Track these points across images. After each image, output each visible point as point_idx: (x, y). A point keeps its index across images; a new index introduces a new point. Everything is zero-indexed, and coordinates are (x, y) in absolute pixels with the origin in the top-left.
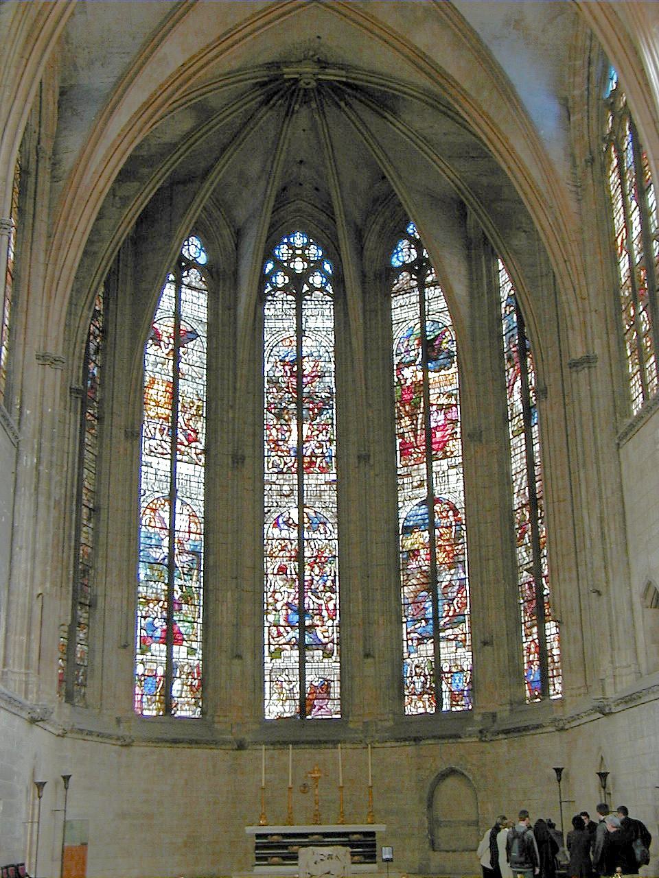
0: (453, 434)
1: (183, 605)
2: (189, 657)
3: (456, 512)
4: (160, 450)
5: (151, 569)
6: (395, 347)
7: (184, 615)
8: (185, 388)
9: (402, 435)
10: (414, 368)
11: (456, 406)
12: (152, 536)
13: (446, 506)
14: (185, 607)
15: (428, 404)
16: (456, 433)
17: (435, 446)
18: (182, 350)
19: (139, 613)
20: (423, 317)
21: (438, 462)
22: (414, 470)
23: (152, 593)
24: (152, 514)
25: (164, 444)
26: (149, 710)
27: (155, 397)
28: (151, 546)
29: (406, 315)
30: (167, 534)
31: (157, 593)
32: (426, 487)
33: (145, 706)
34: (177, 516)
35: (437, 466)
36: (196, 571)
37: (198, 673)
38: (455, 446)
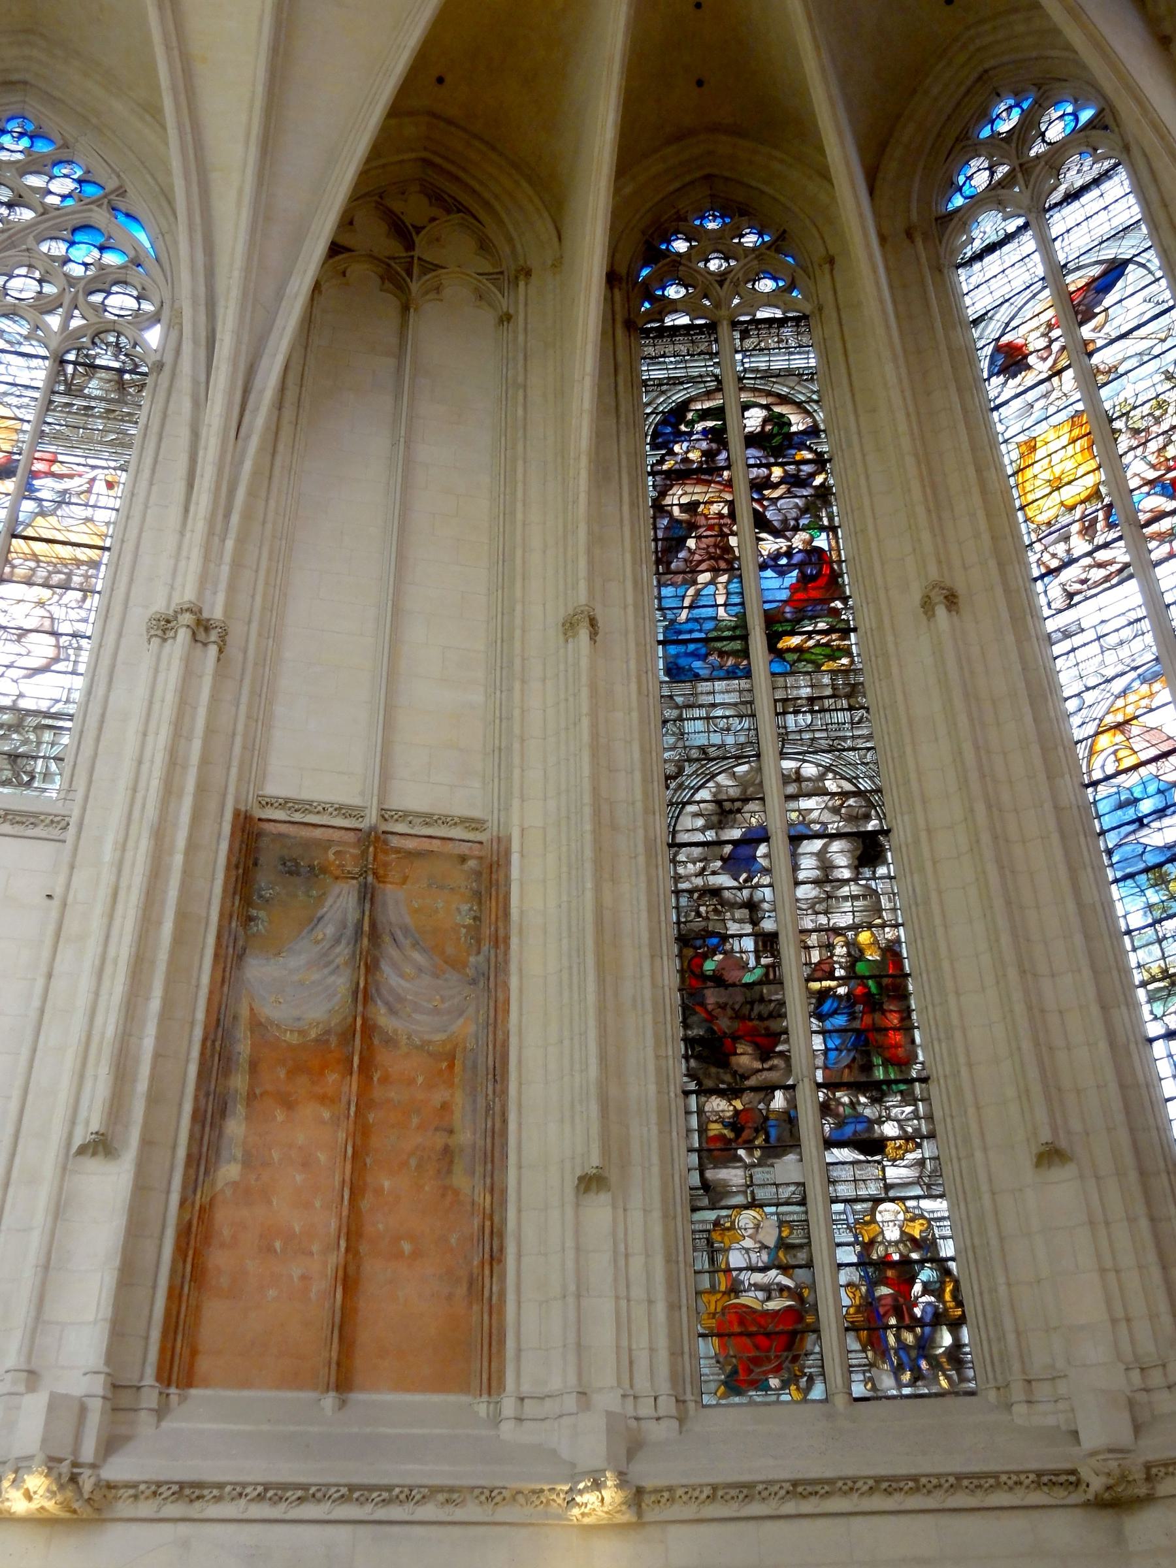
4: (1102, 573)
5: (1162, 881)
8: (1128, 393)
18: (1086, 331)
24: (1120, 738)
25: (1102, 556)
27: (1047, 475)
28: (1140, 822)
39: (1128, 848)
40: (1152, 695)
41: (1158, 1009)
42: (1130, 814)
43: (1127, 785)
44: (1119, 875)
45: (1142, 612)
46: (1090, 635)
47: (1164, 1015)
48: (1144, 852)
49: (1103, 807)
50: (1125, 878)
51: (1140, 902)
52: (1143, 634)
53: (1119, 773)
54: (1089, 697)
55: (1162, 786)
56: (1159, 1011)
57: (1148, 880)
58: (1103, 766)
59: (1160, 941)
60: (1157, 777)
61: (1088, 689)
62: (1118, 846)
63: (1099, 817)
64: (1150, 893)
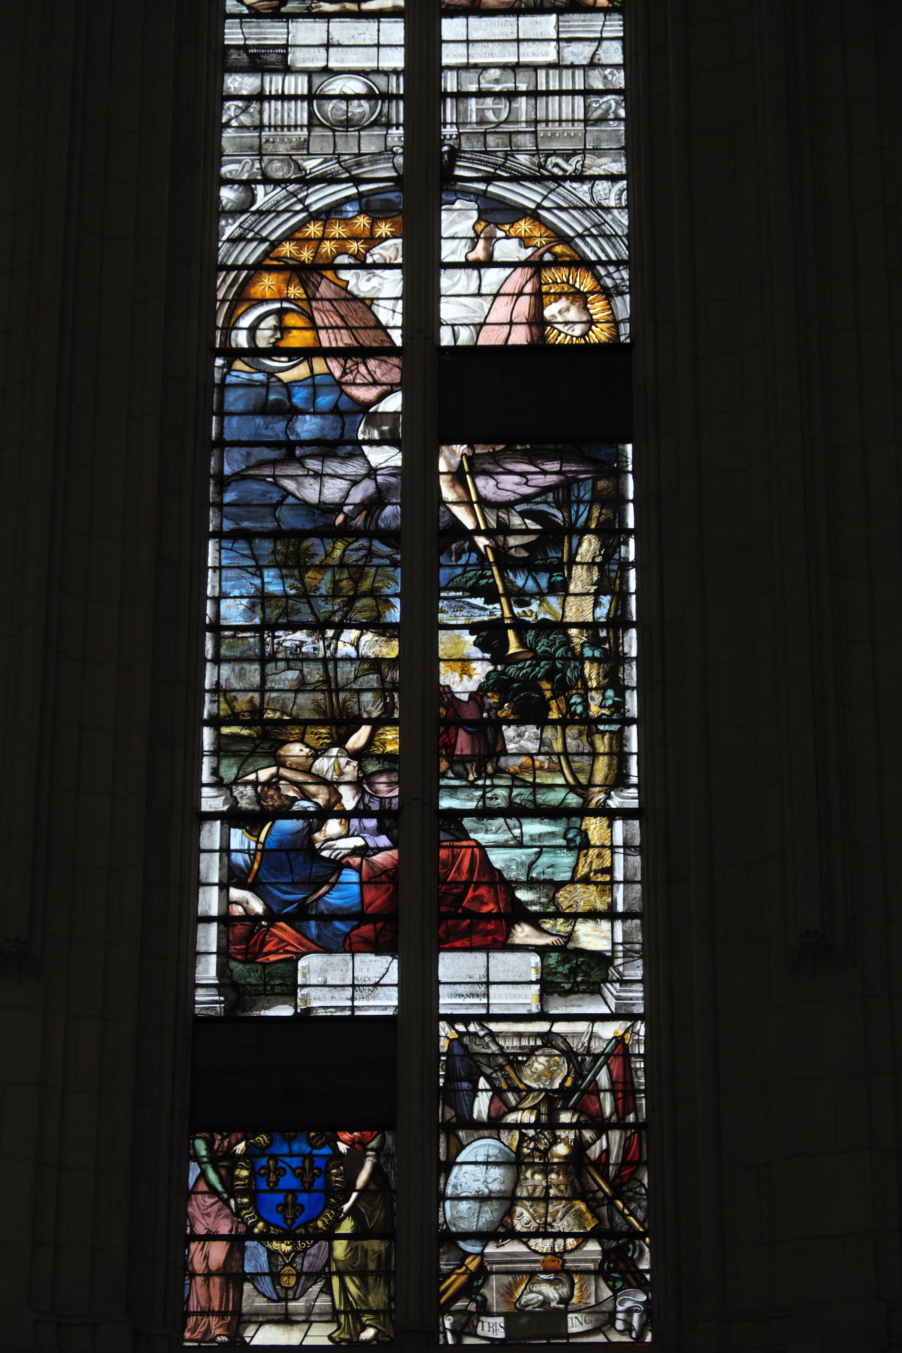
1: (509, 732)
2: (558, 1007)
5: (294, 563)
7: (516, 779)
12: (299, 397)
14: (520, 739)
19: (211, 801)
23: (301, 686)
24: (295, 291)
26: (286, 1320)
28: (290, 451)
30: (395, 376)
31: (329, 685)
33: (252, 1299)
34: (448, 281)
36: (588, 547)
37: (623, 1089)
39: (256, 487)
40: (373, 241)
41: (229, 772)
42: (276, 428)
43: (286, 376)
44: (228, 525)
45: (396, 85)
46: (297, 84)
47: (235, 782)
48: (280, 504)
49: (234, 400)
50: (235, 535)
51: (249, 585)
52: (388, 125)
53: (274, 351)
54: (263, 196)
55: (344, 404)
56: (229, 772)
57: (274, 552)
58: (253, 330)
59: (264, 660)
60: (339, 384)
61: (267, 180)
62: (240, 477)
63: (222, 414)
64: (270, 575)
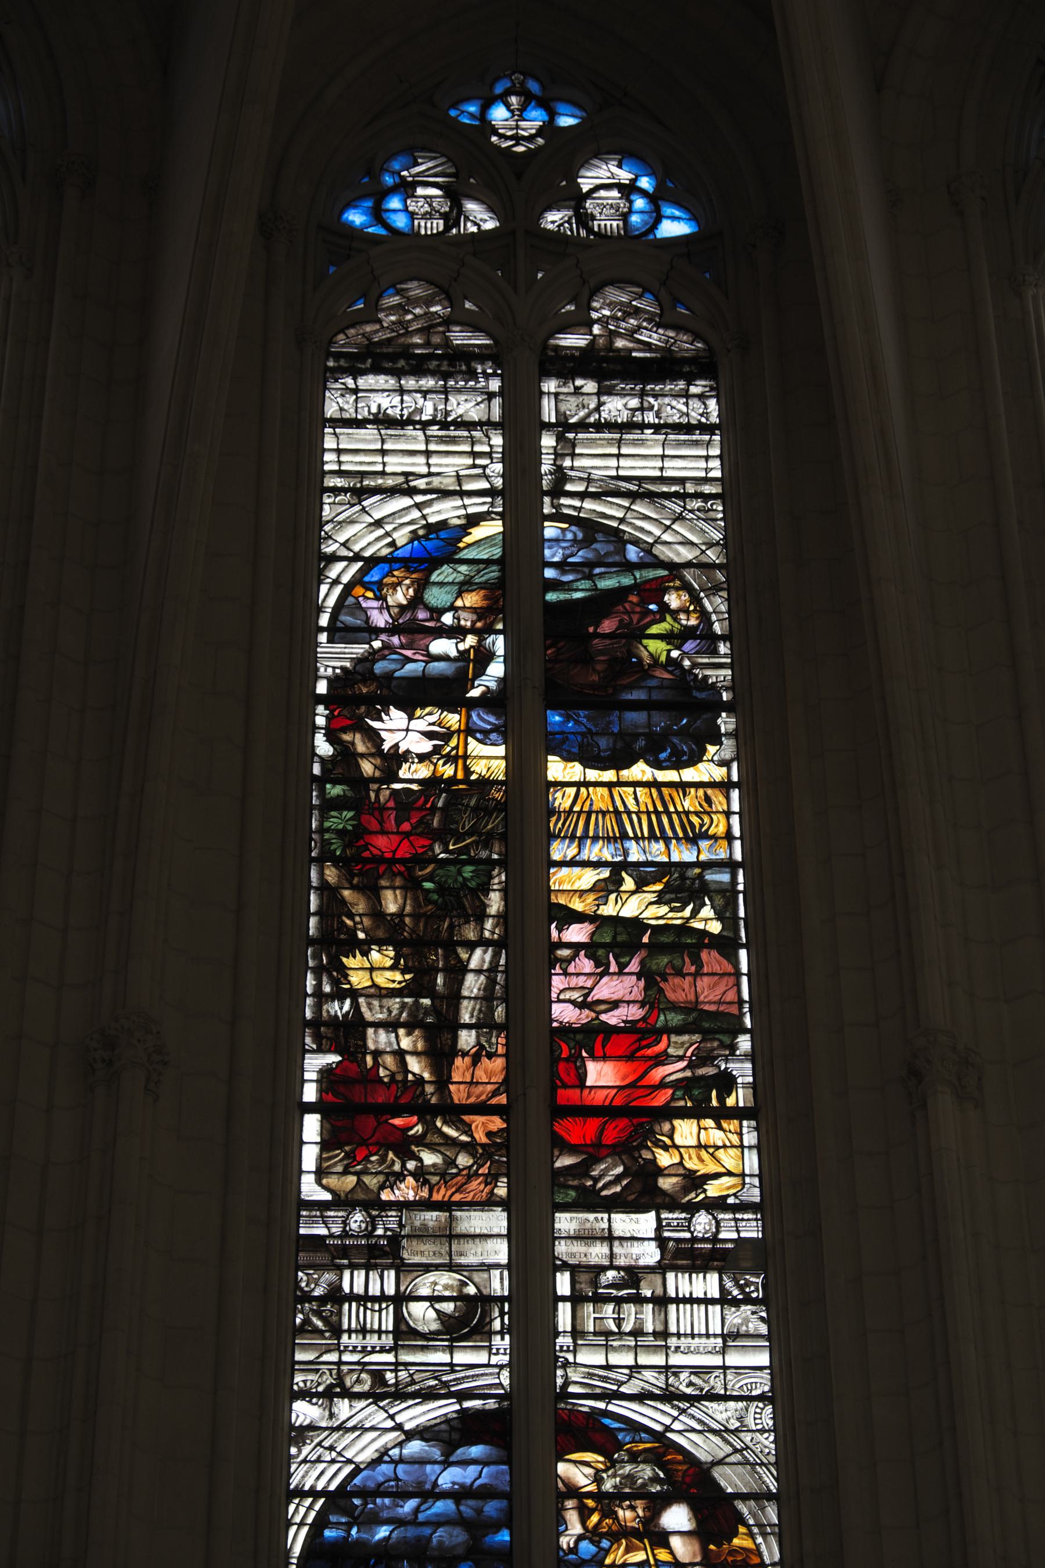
0: (708, 1083)
3: (716, 1515)
6: (329, 596)
9: (347, 1035)
10: (453, 720)
11: (726, 945)
13: (646, 1472)
15: (536, 911)
16: (726, 1083)
17: (570, 1129)
20: (522, 494)
21: (597, 1221)
22: (422, 1234)
29: (418, 465)
32: (502, 1343)
35: (585, 1237)
38: (718, 1152)
